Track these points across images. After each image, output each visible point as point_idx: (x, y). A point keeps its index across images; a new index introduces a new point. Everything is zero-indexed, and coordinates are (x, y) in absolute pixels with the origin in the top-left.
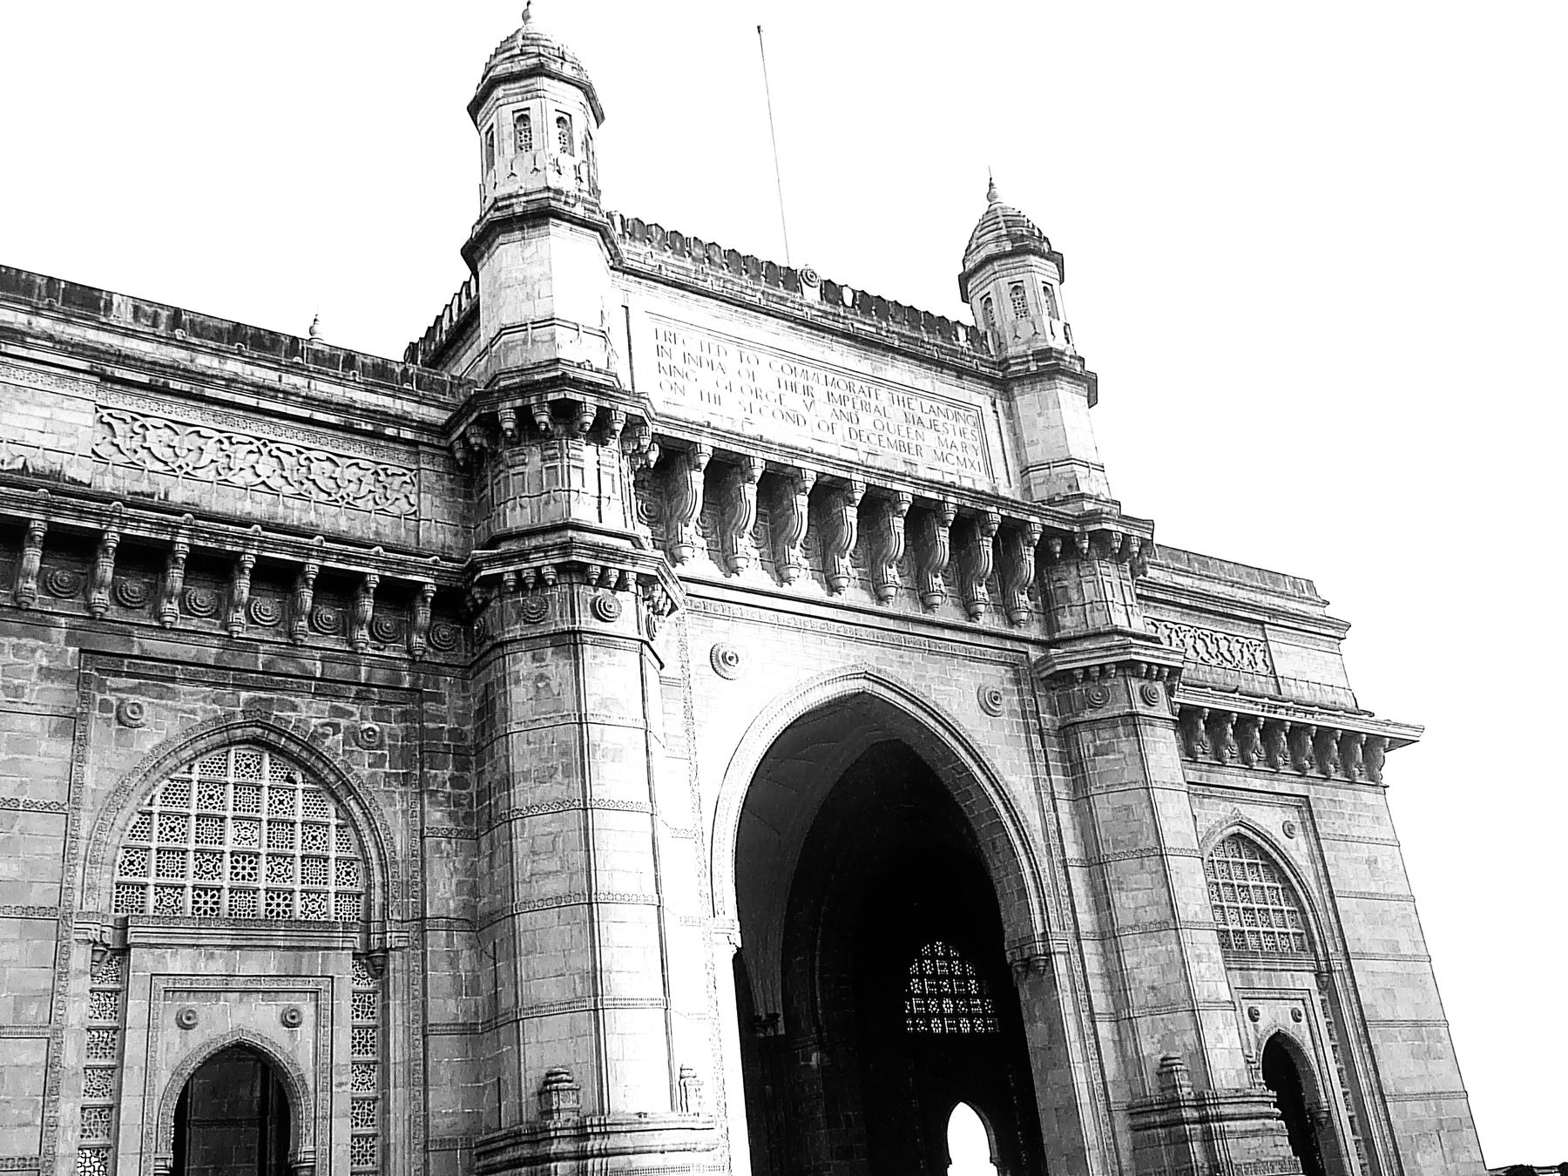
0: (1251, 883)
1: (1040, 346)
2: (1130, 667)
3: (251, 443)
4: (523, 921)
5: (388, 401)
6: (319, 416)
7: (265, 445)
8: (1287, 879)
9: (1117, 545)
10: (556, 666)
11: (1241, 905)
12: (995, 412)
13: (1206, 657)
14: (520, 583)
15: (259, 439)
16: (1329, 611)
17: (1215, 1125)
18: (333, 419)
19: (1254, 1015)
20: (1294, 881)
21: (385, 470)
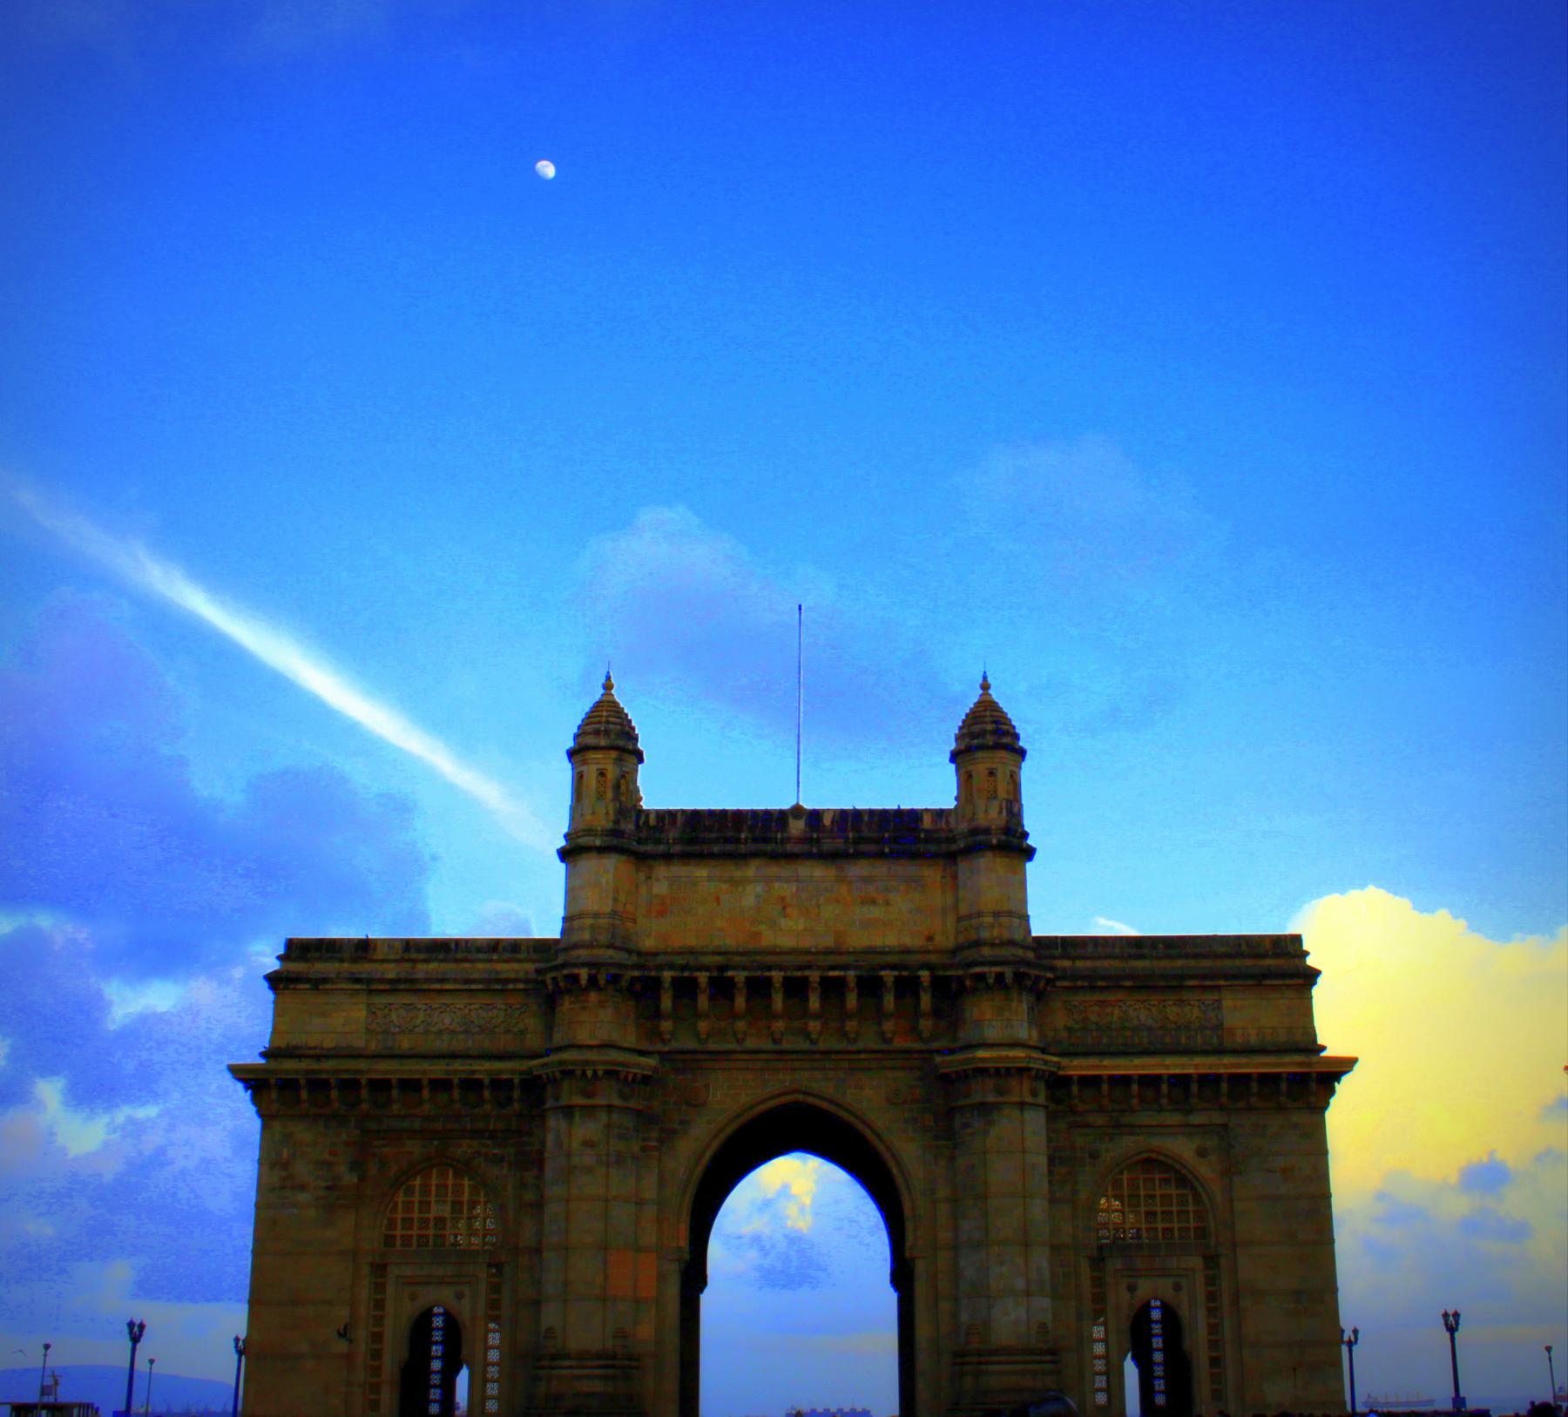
0: (1158, 1192)
1: (975, 823)
2: (982, 1072)
3: (440, 1008)
4: (545, 1254)
5: (516, 966)
6: (473, 987)
7: (448, 1006)
8: (1193, 1188)
9: (991, 981)
10: (563, 1125)
11: (1143, 1209)
12: (943, 877)
13: (1150, 1022)
14: (548, 1079)
15: (444, 1004)
16: (1310, 961)
17: (983, 1367)
18: (480, 987)
19: (1132, 1288)
20: (1200, 1190)
21: (510, 1007)
